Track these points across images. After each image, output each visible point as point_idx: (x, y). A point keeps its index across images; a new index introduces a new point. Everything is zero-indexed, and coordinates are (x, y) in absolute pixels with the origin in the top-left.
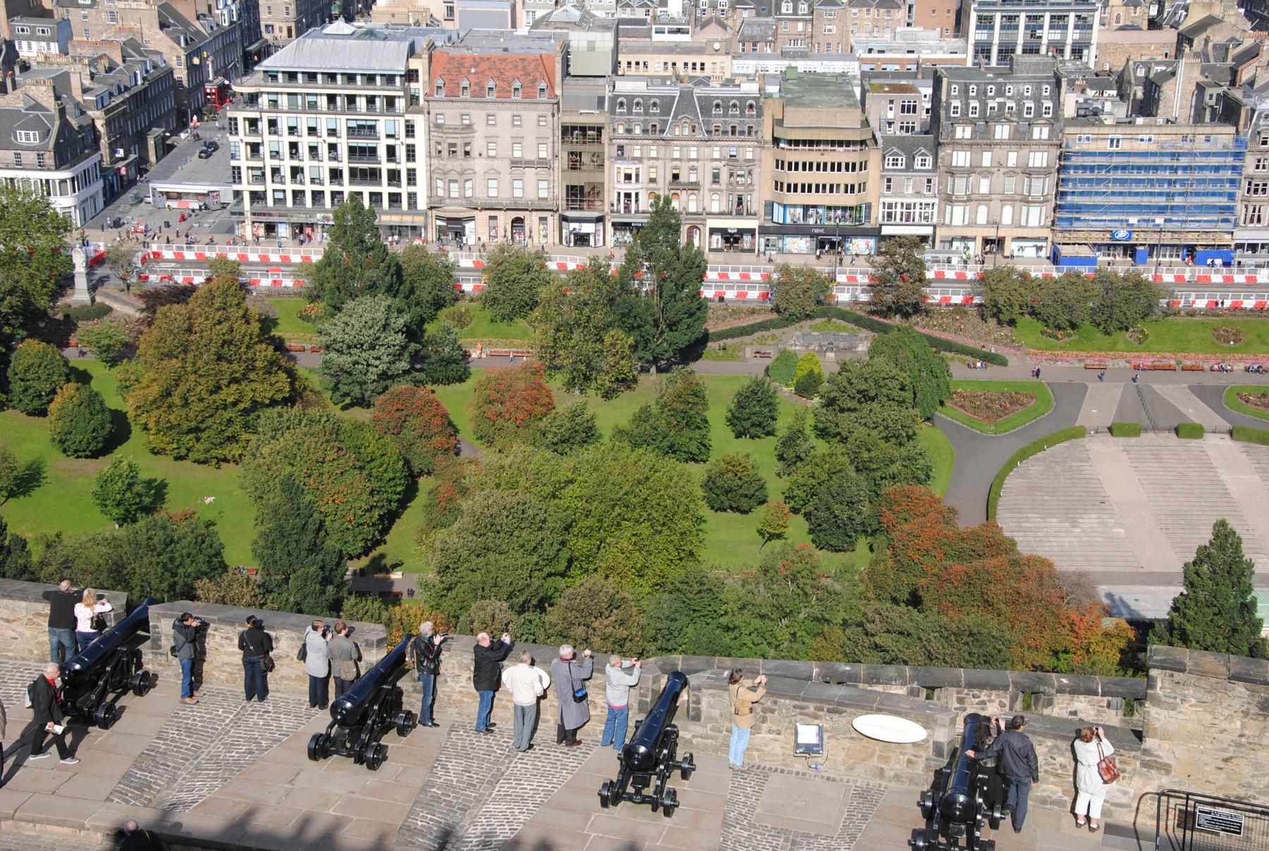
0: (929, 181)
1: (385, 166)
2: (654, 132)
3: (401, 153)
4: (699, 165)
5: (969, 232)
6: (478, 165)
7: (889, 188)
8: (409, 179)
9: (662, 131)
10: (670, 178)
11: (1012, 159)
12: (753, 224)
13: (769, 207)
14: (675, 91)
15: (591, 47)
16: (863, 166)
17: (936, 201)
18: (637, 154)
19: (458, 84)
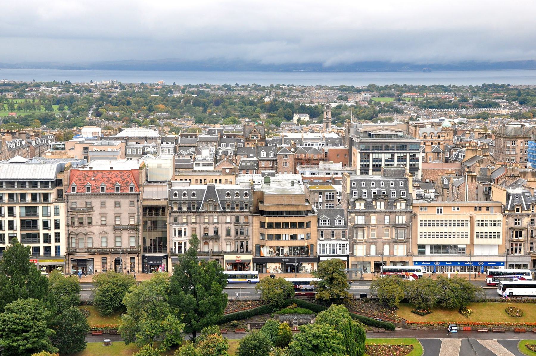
0: (343, 232)
1: (42, 232)
2: (194, 208)
3: (52, 224)
4: (219, 226)
5: (367, 259)
6: (95, 229)
7: (322, 236)
8: (56, 239)
9: (198, 208)
10: (203, 233)
11: (387, 219)
12: (250, 257)
13: (259, 248)
14: (205, 187)
15: (159, 167)
16: (308, 225)
17: (348, 242)
18: (185, 221)
19: (84, 186)
